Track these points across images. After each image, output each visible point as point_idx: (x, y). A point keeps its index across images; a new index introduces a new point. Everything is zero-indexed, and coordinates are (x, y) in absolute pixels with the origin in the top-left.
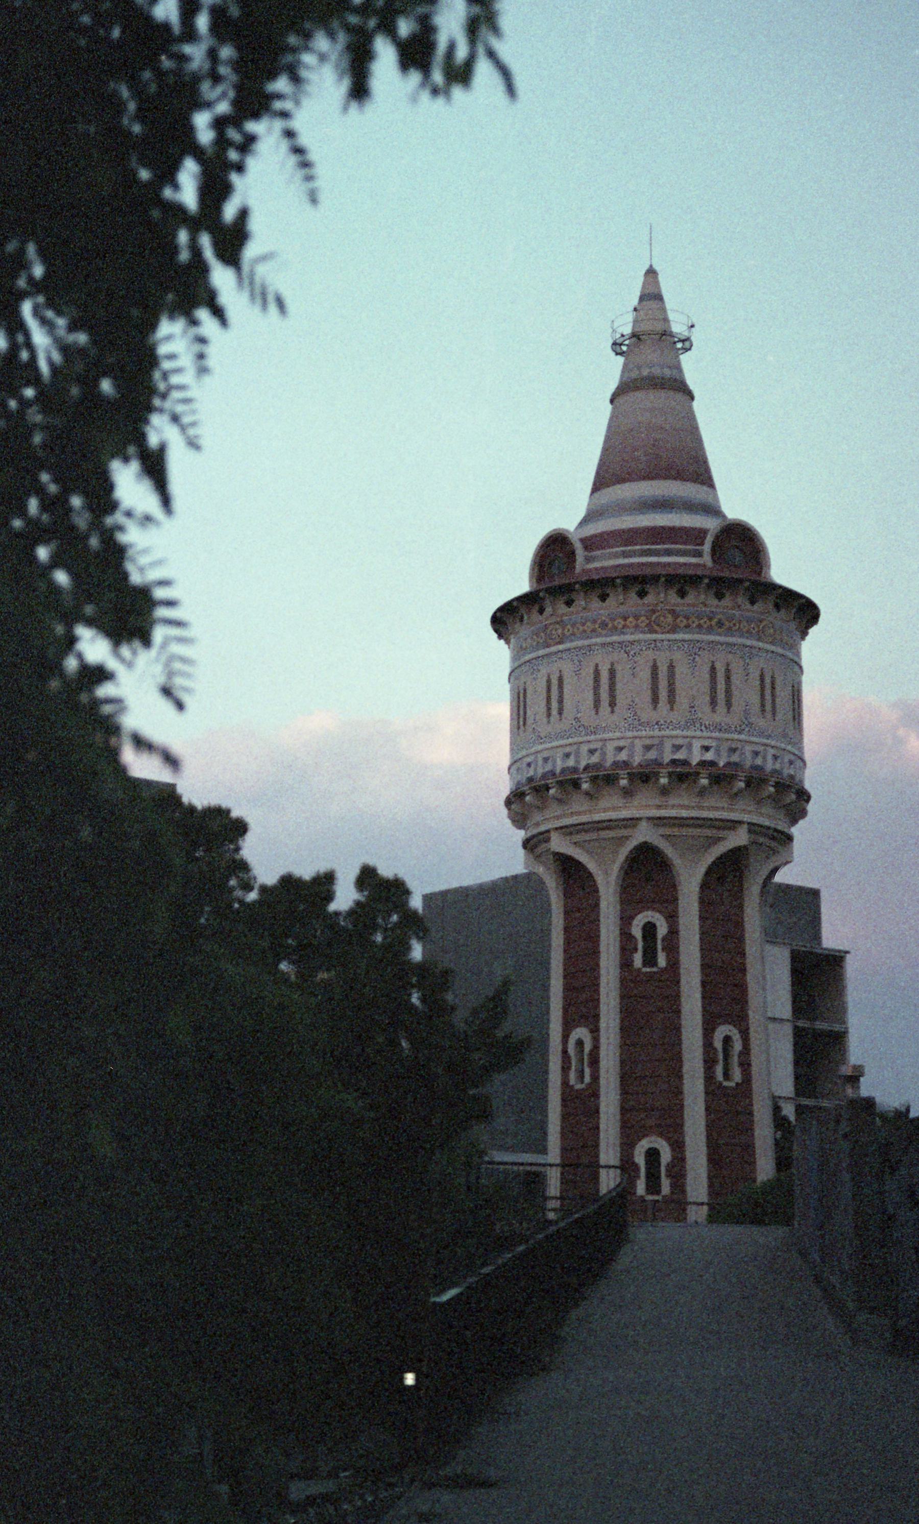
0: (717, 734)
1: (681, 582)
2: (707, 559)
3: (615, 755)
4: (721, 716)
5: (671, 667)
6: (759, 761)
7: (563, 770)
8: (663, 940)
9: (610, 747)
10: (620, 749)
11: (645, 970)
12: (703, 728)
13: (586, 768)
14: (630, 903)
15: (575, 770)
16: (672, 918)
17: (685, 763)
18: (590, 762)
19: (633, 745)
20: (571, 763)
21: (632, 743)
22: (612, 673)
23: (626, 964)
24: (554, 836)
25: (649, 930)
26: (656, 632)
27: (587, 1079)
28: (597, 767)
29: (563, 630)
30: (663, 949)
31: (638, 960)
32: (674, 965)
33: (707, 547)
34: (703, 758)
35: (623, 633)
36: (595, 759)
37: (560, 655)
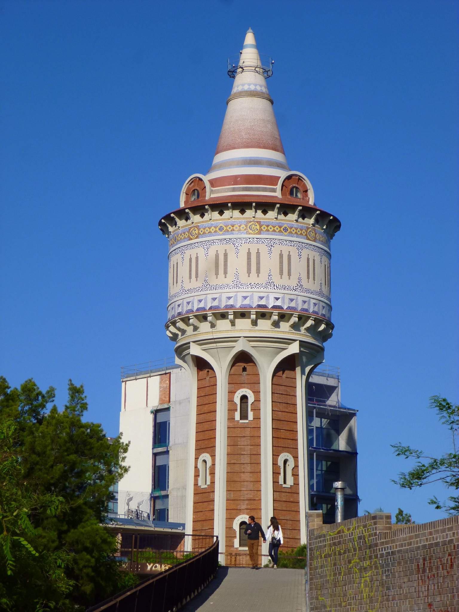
0: (283, 291)
1: (265, 206)
2: (278, 194)
4: (285, 281)
6: (306, 306)
7: (198, 310)
9: (224, 296)
10: (229, 298)
12: (275, 287)
13: (211, 308)
14: (234, 383)
15: (204, 309)
16: (257, 393)
17: (265, 307)
20: (202, 305)
21: (236, 295)
23: (231, 418)
25: (244, 398)
27: (208, 483)
28: (217, 308)
29: (199, 230)
32: (257, 418)
33: (279, 187)
34: (275, 304)
35: (233, 234)
36: (216, 303)
37: (196, 245)
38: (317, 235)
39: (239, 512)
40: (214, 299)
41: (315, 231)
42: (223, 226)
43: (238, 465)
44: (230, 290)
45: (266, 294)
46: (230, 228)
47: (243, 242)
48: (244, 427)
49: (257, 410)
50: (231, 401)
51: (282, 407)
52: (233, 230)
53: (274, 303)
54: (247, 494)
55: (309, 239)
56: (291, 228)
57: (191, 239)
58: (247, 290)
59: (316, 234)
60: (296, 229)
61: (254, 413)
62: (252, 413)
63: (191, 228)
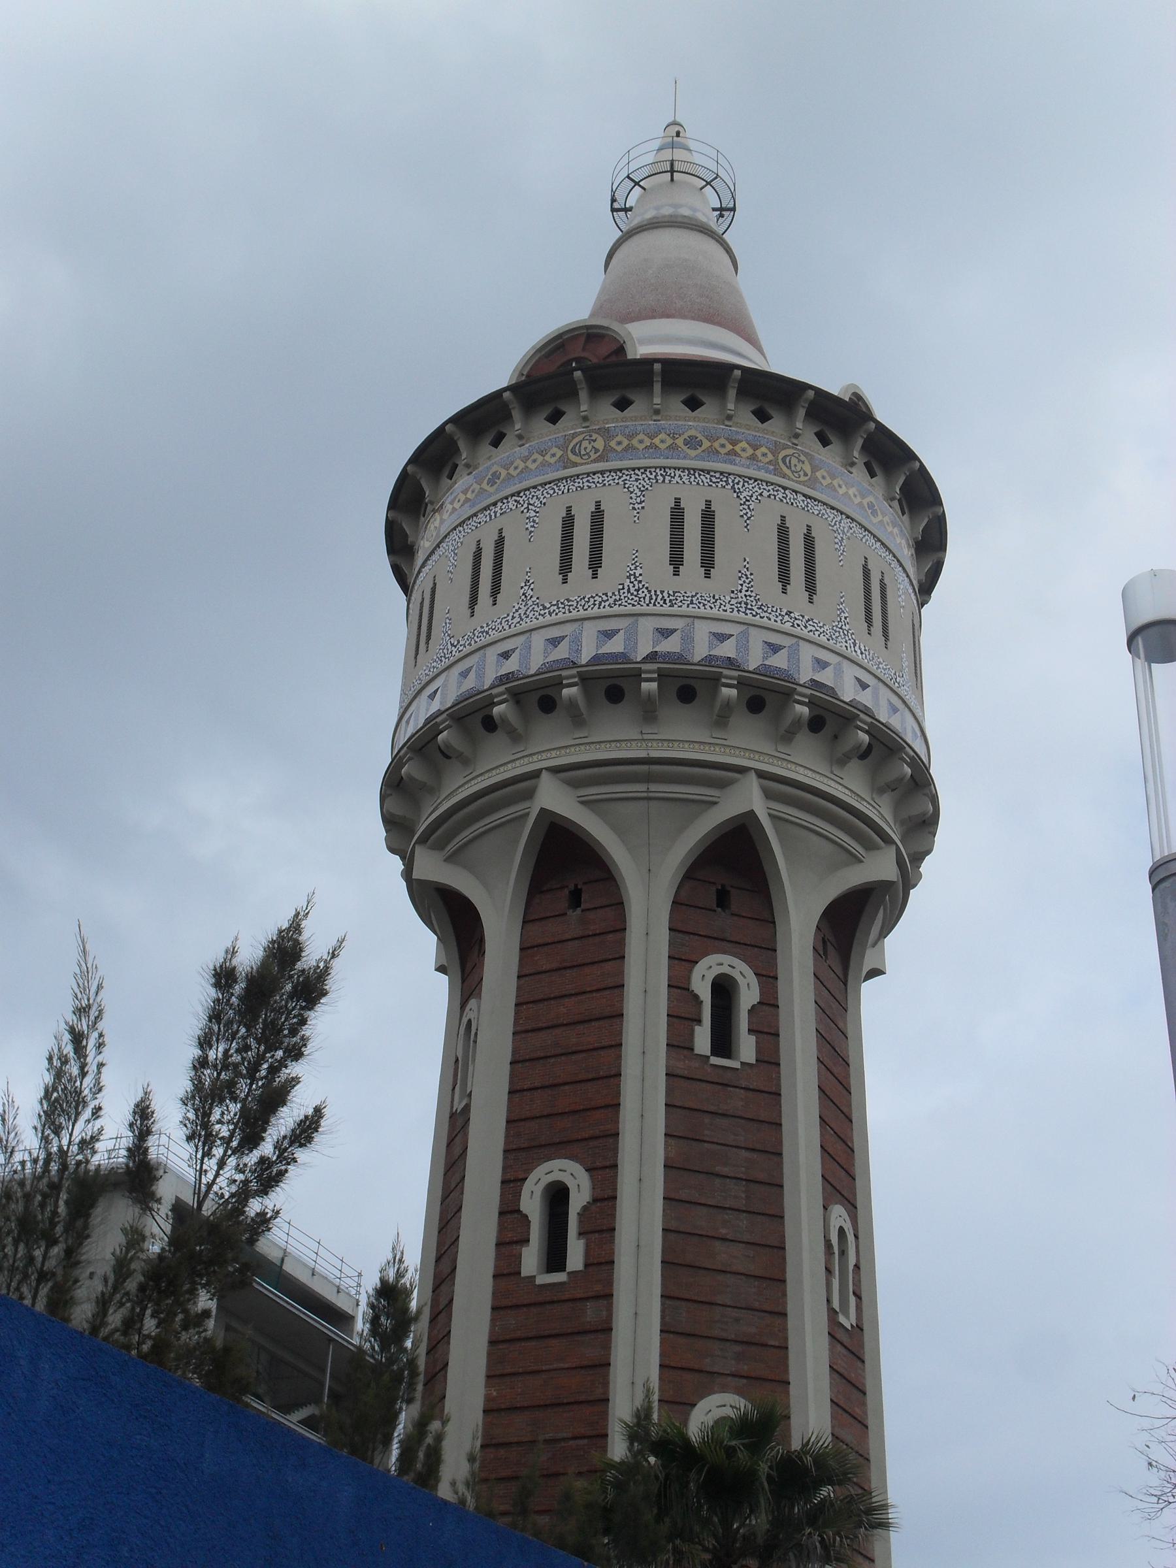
7: (596, 659)
9: (702, 631)
12: (857, 648)
13: (652, 657)
15: (623, 657)
17: (831, 691)
19: (745, 636)
22: (708, 517)
23: (679, 1045)
24: (547, 784)
25: (724, 989)
28: (678, 658)
31: (702, 1039)
32: (769, 1060)
35: (732, 462)
36: (671, 645)
39: (709, 1380)
40: (666, 633)
42: (700, 437)
43: (705, 1210)
47: (766, 494)
49: (768, 1031)
50: (679, 987)
54: (737, 1320)
57: (575, 465)
58: (778, 626)
61: (757, 1042)
63: (574, 436)
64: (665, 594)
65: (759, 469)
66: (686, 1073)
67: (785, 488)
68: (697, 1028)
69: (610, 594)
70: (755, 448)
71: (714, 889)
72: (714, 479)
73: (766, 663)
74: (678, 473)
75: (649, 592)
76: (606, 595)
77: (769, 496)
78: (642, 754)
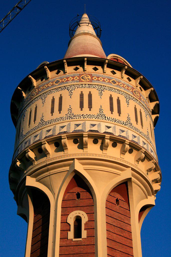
3: (60, 130)
5: (90, 96)
8: (85, 224)
9: (58, 126)
11: (74, 240)
13: (46, 137)
18: (46, 136)
19: (69, 124)
23: (64, 238)
25: (78, 220)
26: (82, 81)
30: (85, 229)
31: (71, 235)
38: (141, 97)
40: (49, 131)
41: (140, 93)
44: (63, 121)
45: (99, 122)
46: (65, 80)
47: (76, 87)
48: (78, 245)
50: (64, 222)
51: (116, 230)
52: (68, 80)
53: (106, 130)
55: (134, 95)
56: (119, 82)
58: (79, 119)
59: (140, 96)
60: (124, 85)
61: (87, 232)
62: (86, 231)
64: (49, 121)
65: (75, 82)
66: (66, 245)
67: (82, 84)
68: (69, 232)
69: (37, 126)
70: (73, 77)
71: (75, 194)
72: (62, 89)
73: (75, 130)
74: (53, 90)
75: (45, 122)
76: (36, 127)
77: (77, 88)
78: (45, 164)
